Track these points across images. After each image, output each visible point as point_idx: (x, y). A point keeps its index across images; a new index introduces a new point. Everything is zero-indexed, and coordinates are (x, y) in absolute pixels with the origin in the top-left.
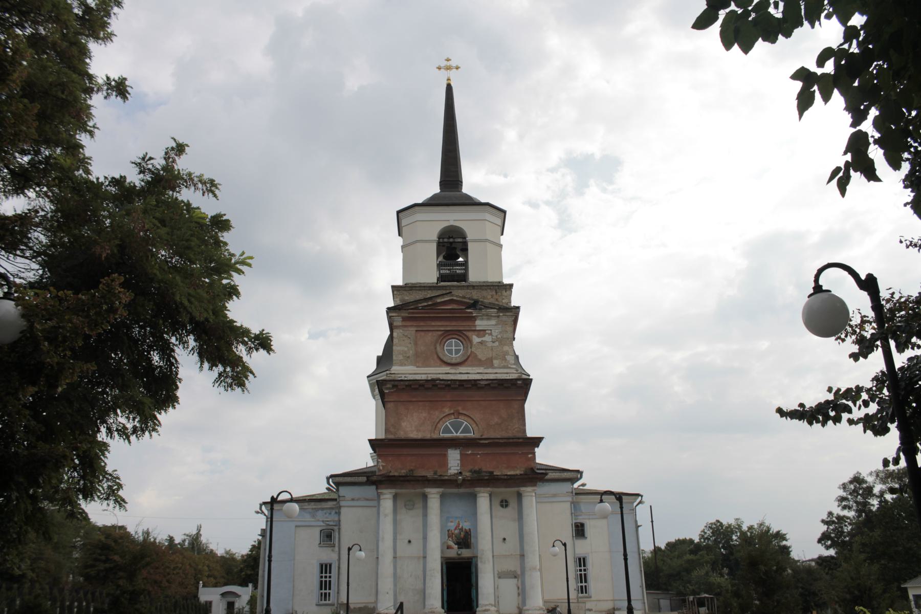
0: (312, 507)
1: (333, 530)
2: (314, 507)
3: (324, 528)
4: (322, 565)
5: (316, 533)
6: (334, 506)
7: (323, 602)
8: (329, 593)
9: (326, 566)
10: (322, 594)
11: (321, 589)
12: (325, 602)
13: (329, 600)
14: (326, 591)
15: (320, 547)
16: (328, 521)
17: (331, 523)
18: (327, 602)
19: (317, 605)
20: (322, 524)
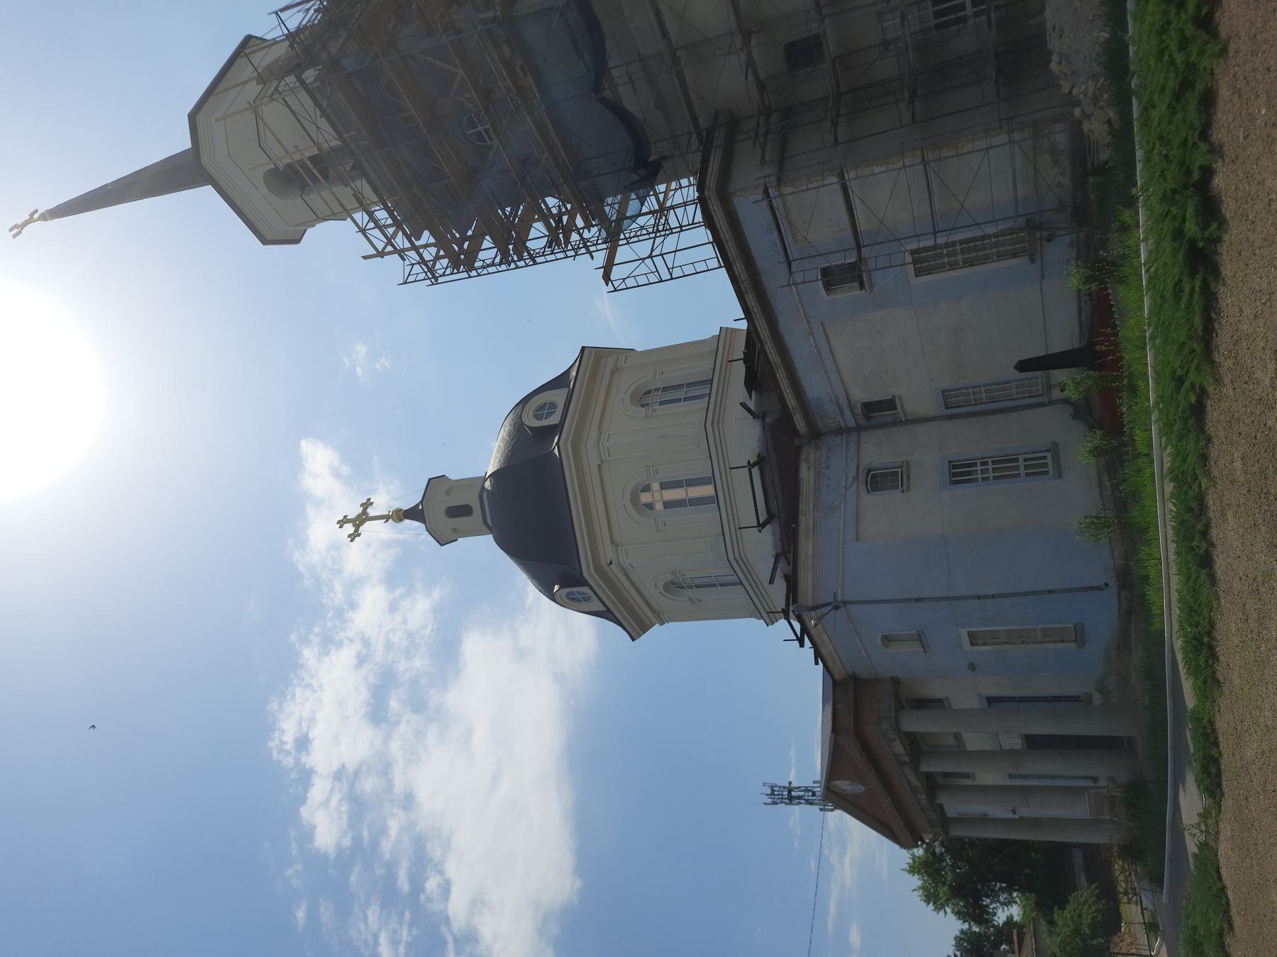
0: (811, 511)
1: (869, 471)
2: (811, 506)
3: (862, 487)
4: (956, 482)
5: (873, 502)
6: (812, 469)
7: (1050, 468)
8: (1025, 460)
9: (955, 475)
10: (1027, 475)
11: (1018, 475)
12: (1050, 464)
13: (1045, 458)
14: (1022, 468)
15: (908, 489)
16: (847, 479)
17: (852, 472)
18: (1049, 461)
19: (1060, 476)
20: (854, 489)
